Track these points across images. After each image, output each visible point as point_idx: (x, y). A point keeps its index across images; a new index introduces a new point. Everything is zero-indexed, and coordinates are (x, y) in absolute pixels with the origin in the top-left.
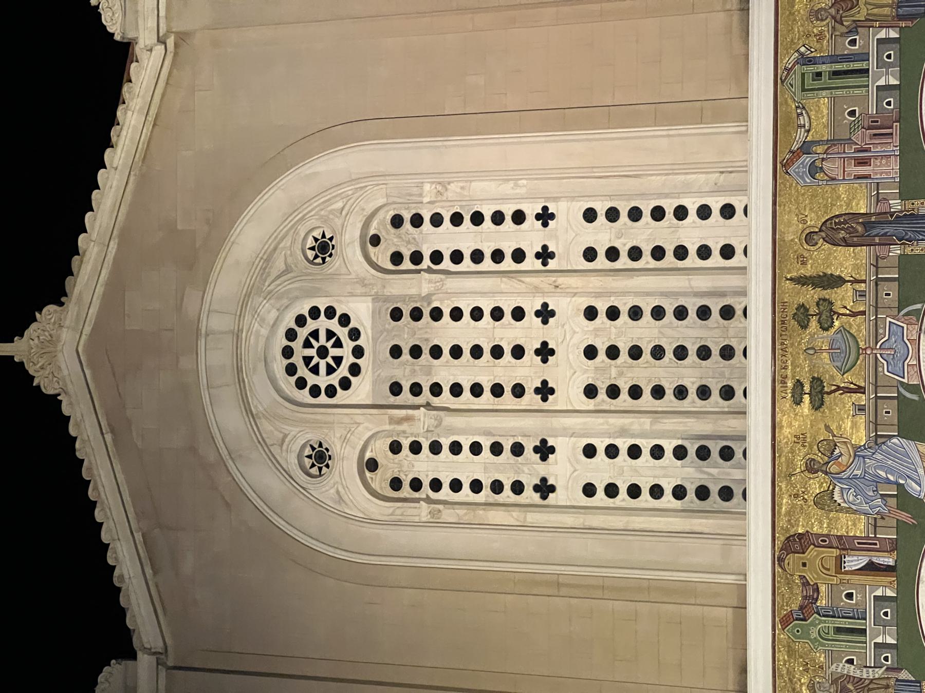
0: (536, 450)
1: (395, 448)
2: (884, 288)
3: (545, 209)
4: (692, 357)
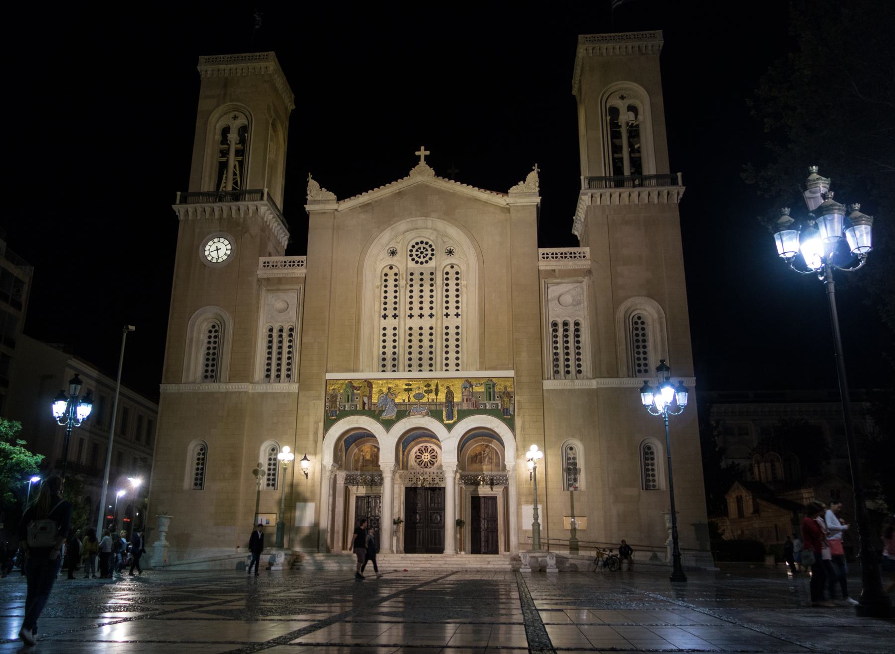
0: (395, 314)
1: (396, 274)
2: (435, 406)
3: (460, 315)
4: (419, 356)
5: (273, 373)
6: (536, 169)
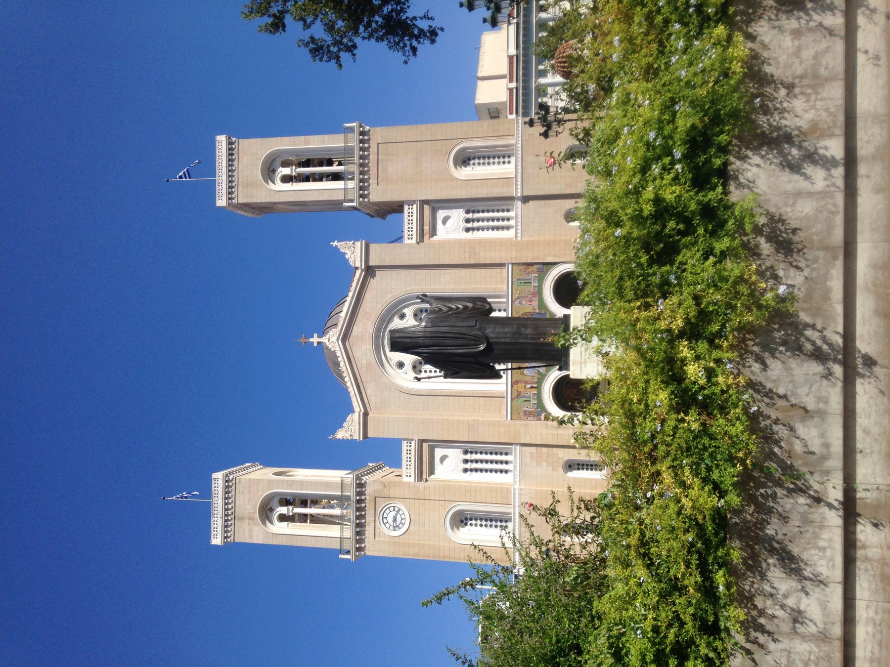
5: (503, 467)
6: (335, 243)
